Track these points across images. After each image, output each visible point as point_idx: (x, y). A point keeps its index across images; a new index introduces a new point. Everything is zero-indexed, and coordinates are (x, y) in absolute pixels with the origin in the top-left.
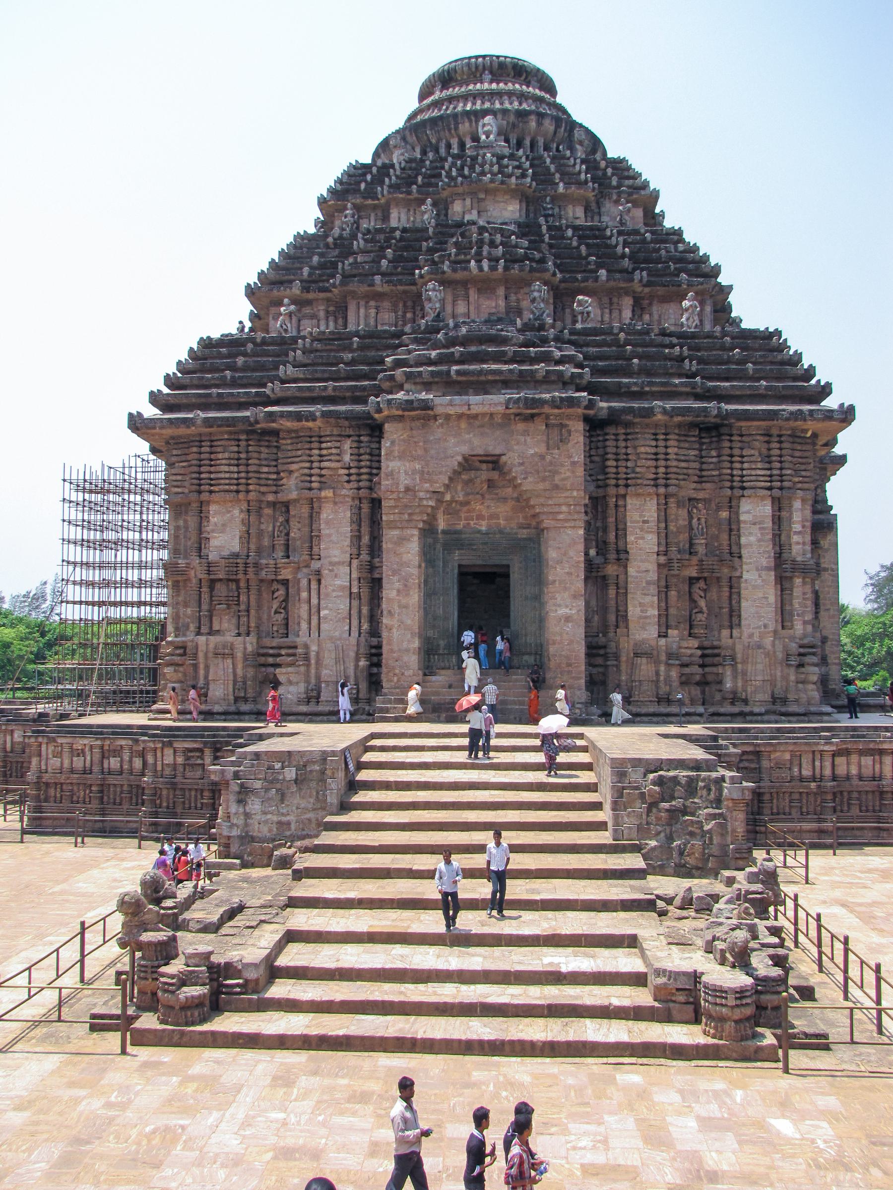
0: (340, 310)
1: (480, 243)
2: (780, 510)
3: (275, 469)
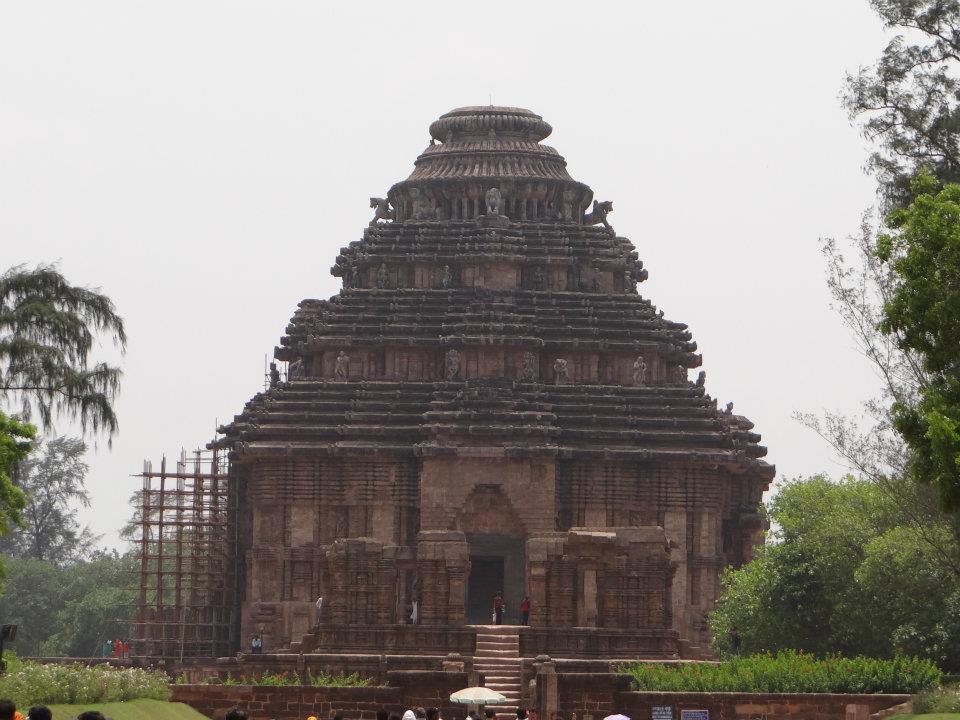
0: (379, 355)
1: (487, 319)
2: (693, 520)
3: (338, 483)
